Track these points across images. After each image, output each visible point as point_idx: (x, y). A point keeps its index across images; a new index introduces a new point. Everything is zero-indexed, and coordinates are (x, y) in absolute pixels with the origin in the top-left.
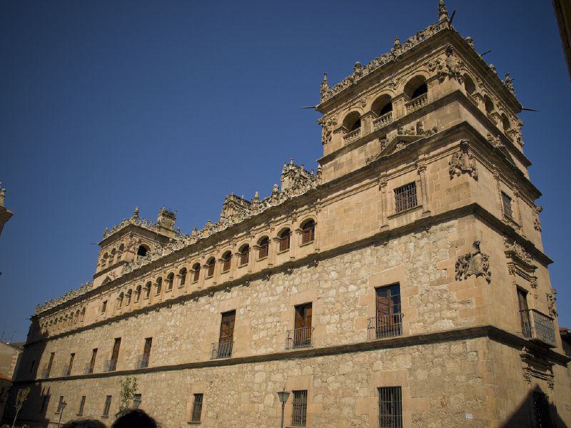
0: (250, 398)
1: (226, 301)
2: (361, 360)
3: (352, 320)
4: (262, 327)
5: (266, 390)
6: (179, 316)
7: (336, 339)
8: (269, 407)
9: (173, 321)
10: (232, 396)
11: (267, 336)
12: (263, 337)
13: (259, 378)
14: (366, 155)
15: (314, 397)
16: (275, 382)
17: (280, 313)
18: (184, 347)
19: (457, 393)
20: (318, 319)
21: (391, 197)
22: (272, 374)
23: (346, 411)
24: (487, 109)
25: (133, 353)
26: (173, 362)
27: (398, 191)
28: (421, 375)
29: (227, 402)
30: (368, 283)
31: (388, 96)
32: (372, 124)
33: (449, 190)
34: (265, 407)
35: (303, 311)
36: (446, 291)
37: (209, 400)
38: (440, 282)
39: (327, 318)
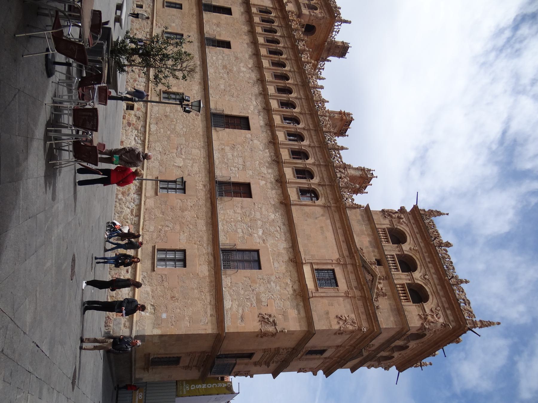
1: (257, 121)
3: (236, 231)
4: (235, 154)
6: (248, 76)
7: (223, 218)
9: (244, 69)
14: (367, 247)
16: (192, 167)
18: (222, 82)
19: (180, 309)
21: (329, 267)
24: (396, 346)
25: (218, 29)
26: (211, 71)
27: (333, 270)
30: (263, 245)
31: (415, 269)
32: (394, 254)
33: (327, 313)
35: (244, 190)
36: (252, 304)
38: (259, 301)
39: (239, 211)
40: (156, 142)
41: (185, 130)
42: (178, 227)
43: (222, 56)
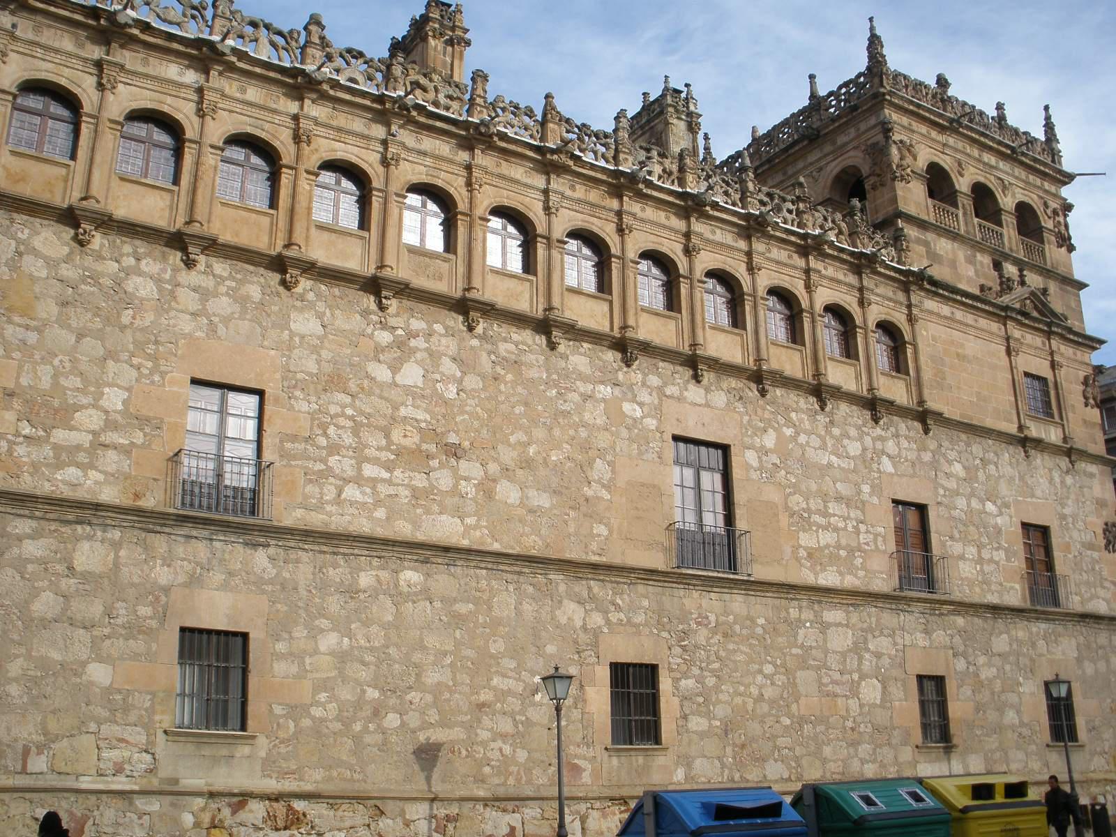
0: (821, 684)
2: (1021, 634)
3: (997, 563)
4: (816, 518)
5: (859, 670)
7: (977, 590)
8: (874, 706)
10: (765, 676)
11: (839, 546)
12: (827, 546)
13: (840, 640)
15: (959, 687)
16: (878, 655)
17: (863, 503)
20: (943, 545)
22: (870, 636)
23: (1011, 716)
28: (1089, 669)
29: (754, 691)
33: (1085, 421)
34: (861, 706)
37: (688, 684)
40: (824, 761)
41: (768, 669)
42: (1013, 698)
43: (334, 449)
